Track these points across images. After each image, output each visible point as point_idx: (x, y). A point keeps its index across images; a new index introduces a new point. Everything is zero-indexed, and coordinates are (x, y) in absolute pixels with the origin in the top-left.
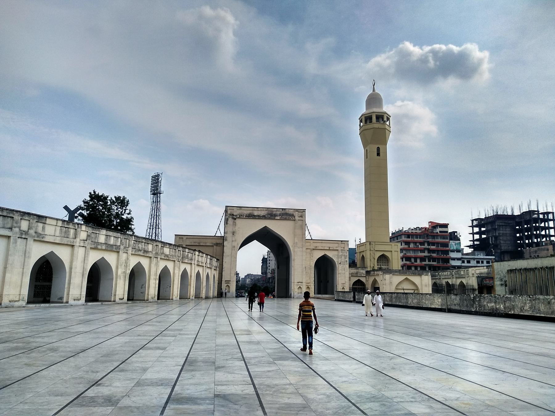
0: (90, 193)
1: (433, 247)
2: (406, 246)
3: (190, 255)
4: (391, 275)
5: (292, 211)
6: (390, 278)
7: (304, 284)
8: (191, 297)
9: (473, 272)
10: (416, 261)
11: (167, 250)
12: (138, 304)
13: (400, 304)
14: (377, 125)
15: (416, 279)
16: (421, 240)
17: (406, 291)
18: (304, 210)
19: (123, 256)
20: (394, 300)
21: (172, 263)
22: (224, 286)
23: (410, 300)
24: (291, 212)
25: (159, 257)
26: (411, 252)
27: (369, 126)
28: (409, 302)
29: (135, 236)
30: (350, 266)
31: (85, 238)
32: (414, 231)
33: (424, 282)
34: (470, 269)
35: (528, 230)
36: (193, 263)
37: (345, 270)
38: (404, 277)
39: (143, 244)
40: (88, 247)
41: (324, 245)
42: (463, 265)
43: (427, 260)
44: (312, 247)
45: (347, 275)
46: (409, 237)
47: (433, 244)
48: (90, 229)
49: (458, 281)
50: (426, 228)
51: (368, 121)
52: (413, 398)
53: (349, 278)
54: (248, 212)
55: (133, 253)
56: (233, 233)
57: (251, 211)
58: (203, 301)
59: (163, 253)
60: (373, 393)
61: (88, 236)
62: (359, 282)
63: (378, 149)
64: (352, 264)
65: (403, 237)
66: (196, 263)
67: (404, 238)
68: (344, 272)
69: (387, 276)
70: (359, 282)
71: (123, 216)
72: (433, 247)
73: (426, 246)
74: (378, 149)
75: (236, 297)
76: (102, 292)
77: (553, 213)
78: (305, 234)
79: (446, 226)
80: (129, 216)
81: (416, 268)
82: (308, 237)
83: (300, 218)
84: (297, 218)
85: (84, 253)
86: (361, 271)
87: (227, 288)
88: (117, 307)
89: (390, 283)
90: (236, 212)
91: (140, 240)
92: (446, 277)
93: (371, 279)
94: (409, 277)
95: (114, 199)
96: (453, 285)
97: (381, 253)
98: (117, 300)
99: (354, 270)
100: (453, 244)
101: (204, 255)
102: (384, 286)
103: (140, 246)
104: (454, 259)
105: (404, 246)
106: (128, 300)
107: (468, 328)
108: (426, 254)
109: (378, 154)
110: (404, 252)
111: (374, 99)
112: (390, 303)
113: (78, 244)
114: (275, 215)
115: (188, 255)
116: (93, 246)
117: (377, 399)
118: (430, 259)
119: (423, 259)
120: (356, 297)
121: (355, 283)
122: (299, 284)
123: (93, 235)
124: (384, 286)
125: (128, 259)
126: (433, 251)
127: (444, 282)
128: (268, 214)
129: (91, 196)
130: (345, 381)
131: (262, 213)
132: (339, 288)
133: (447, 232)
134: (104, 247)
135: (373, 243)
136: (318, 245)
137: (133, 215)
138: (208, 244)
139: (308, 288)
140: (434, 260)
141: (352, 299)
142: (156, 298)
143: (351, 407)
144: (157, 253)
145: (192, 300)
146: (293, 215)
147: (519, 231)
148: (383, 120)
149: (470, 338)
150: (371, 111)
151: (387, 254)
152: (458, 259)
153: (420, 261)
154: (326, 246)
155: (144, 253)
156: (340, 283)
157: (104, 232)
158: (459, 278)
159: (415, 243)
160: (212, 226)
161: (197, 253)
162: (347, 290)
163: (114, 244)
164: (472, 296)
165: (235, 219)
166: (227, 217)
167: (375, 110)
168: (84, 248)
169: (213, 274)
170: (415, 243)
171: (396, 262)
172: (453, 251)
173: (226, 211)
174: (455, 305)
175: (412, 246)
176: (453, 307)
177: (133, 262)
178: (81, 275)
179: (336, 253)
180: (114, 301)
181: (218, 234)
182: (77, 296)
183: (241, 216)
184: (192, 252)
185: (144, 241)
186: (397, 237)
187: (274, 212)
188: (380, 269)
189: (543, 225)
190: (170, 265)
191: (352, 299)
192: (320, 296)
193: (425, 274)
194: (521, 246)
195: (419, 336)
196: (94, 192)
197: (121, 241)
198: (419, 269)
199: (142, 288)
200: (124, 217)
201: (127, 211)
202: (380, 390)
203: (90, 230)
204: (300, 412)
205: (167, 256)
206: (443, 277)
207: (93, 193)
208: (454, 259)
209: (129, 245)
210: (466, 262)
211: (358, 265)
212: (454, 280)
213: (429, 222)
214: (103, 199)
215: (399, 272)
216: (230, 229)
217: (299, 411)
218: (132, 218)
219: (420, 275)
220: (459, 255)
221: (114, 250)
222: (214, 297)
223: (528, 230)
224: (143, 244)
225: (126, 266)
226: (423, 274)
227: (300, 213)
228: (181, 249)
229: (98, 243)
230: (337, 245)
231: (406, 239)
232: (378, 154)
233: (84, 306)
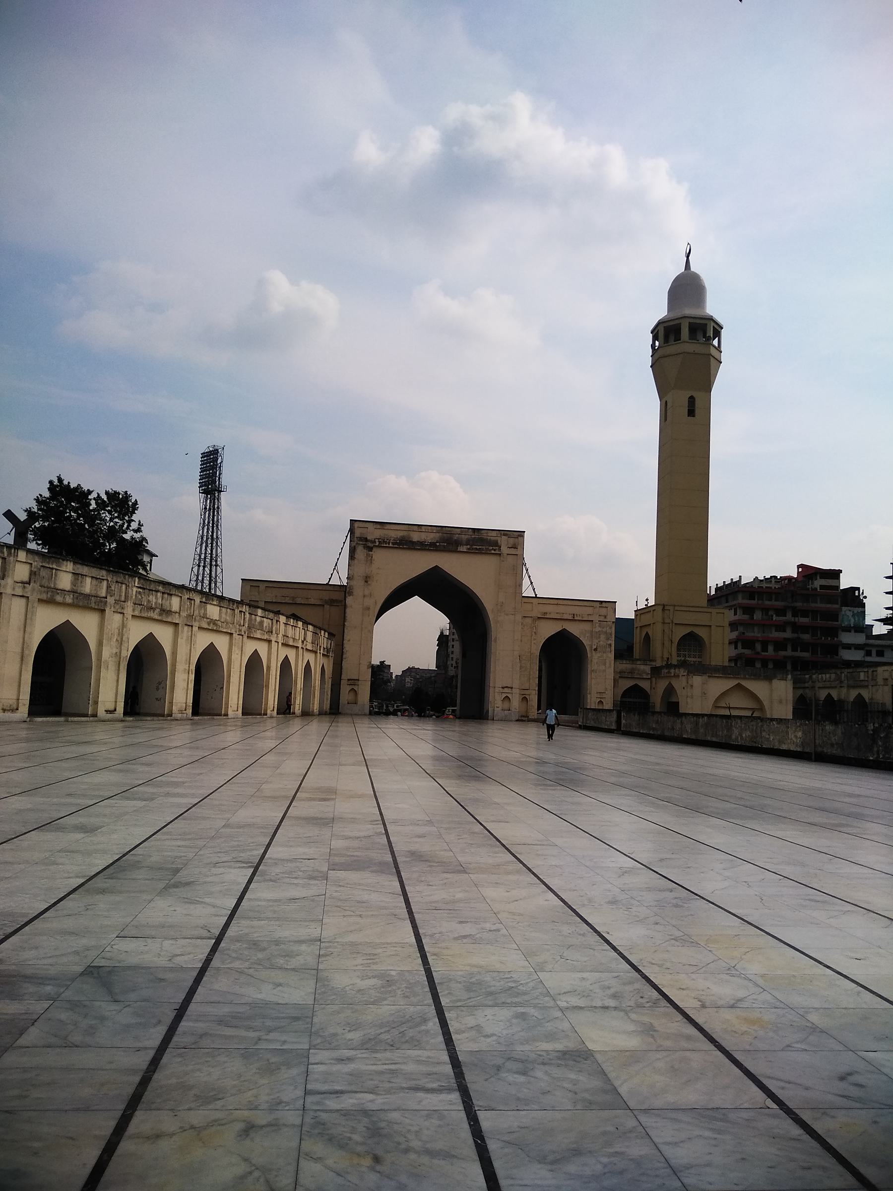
0: (51, 482)
1: (804, 620)
2: (746, 617)
3: (266, 622)
4: (705, 677)
5: (494, 534)
6: (703, 684)
7: (516, 691)
8: (269, 712)
9: (886, 675)
10: (765, 649)
11: (213, 611)
12: (149, 723)
13: (714, 739)
14: (691, 347)
15: (758, 687)
16: (779, 604)
17: (735, 713)
18: (521, 534)
19: (114, 620)
20: (702, 730)
21: (226, 638)
22: (345, 689)
23: (736, 732)
24: (492, 537)
25: (196, 625)
26: (756, 629)
27: (673, 348)
28: (734, 737)
29: (141, 577)
30: (619, 656)
31: (26, 579)
32: (764, 585)
33: (777, 695)
34: (880, 669)
36: (273, 639)
37: (605, 664)
38: (731, 683)
39: (159, 594)
40: (34, 597)
41: (561, 609)
42: (868, 659)
43: (789, 648)
44: (536, 613)
45: (610, 674)
46: (752, 597)
47: (805, 613)
48: (37, 558)
49: (853, 694)
50: (789, 579)
51: (672, 338)
52: (614, 996)
53: (615, 681)
54: (400, 534)
55: (137, 613)
56: (367, 579)
57: (405, 533)
58: (270, 720)
59: (205, 616)
60: (515, 976)
61: (32, 574)
62: (635, 691)
63: (692, 400)
64: (623, 652)
65: (740, 596)
66: (280, 641)
67: (740, 600)
68: (602, 668)
69: (697, 680)
70: (635, 691)
71: (124, 536)
72: (804, 620)
73: (789, 617)
74: (692, 400)
75: (319, 714)
76: (70, 697)
78: (521, 585)
79: (835, 574)
80: (137, 536)
81: (765, 663)
82: (527, 592)
83: (512, 551)
84: (504, 550)
85: (23, 610)
86: (642, 667)
87: (352, 694)
88: (101, 727)
89: (700, 694)
90: (374, 534)
91: (152, 587)
92: (828, 684)
93: (662, 685)
94: (745, 683)
95: (105, 498)
96: (841, 701)
97: (687, 630)
98: (101, 712)
99: (625, 666)
100: (847, 614)
101: (300, 624)
102: (689, 700)
103: (152, 598)
104: (848, 647)
105: (740, 616)
106: (126, 713)
107: (847, 800)
108: (788, 634)
109: (691, 413)
110: (741, 629)
111: (687, 288)
112: (693, 737)
113: (9, 591)
114: (458, 543)
115: (261, 623)
116: (44, 596)
117: (518, 995)
118: (797, 644)
119: (780, 645)
120: (623, 722)
121: (627, 693)
122: (506, 690)
123: (43, 573)
124: (689, 700)
125: (123, 625)
126: (805, 629)
127: (822, 695)
128: (442, 540)
129: (52, 487)
130: (465, 937)
131: (430, 537)
132: (592, 702)
133: (838, 587)
134: (69, 599)
135: (671, 608)
136: (549, 609)
137: (145, 533)
138: (312, 601)
139: (525, 699)
140: (805, 647)
141: (614, 727)
142: (190, 711)
143: (425, 1021)
144: (190, 616)
145: (271, 717)
146: (496, 544)
148: (705, 336)
149: (837, 825)
150: (677, 314)
151: (697, 631)
152: (858, 647)
153: (775, 650)
154: (567, 612)
155: (160, 615)
157: (69, 566)
158: (854, 687)
159: (765, 610)
160: (323, 562)
161: (283, 619)
162: (608, 705)
163: (93, 593)
164: (871, 727)
165: (371, 549)
166: (354, 544)
167: (688, 312)
168: (23, 601)
169: (318, 662)
170: (765, 610)
171: (720, 650)
172: (848, 629)
173: (352, 531)
174: (832, 745)
175: (758, 616)
176: (828, 750)
177: (137, 632)
178: (18, 659)
179: (587, 627)
180: (95, 715)
181: (335, 581)
182: (11, 702)
183: (383, 543)
184: (271, 615)
185: (160, 588)
186: (727, 595)
187: (456, 537)
188: (683, 664)
190: (221, 643)
191: (614, 727)
195: (723, 816)
196: (60, 480)
197: (108, 587)
198: (771, 666)
199: (158, 689)
200: (127, 536)
201: (134, 525)
202: (540, 968)
203: (37, 562)
204: (272, 1036)
205: (214, 622)
206: (820, 685)
207: (56, 482)
208: (848, 647)
209: (126, 597)
210: (874, 653)
211: (636, 655)
212: (844, 690)
213: (799, 567)
214: (80, 495)
215: (722, 672)
216: (361, 570)
217: (270, 1031)
218: (144, 539)
219: (769, 679)
220: (860, 639)
221: (93, 605)
222: (321, 713)
224: (159, 594)
225: (120, 642)
226: (775, 677)
227: (511, 541)
228: (244, 608)
229: (56, 591)
230: (589, 610)
231: (745, 601)
232: (691, 413)
233: (24, 725)
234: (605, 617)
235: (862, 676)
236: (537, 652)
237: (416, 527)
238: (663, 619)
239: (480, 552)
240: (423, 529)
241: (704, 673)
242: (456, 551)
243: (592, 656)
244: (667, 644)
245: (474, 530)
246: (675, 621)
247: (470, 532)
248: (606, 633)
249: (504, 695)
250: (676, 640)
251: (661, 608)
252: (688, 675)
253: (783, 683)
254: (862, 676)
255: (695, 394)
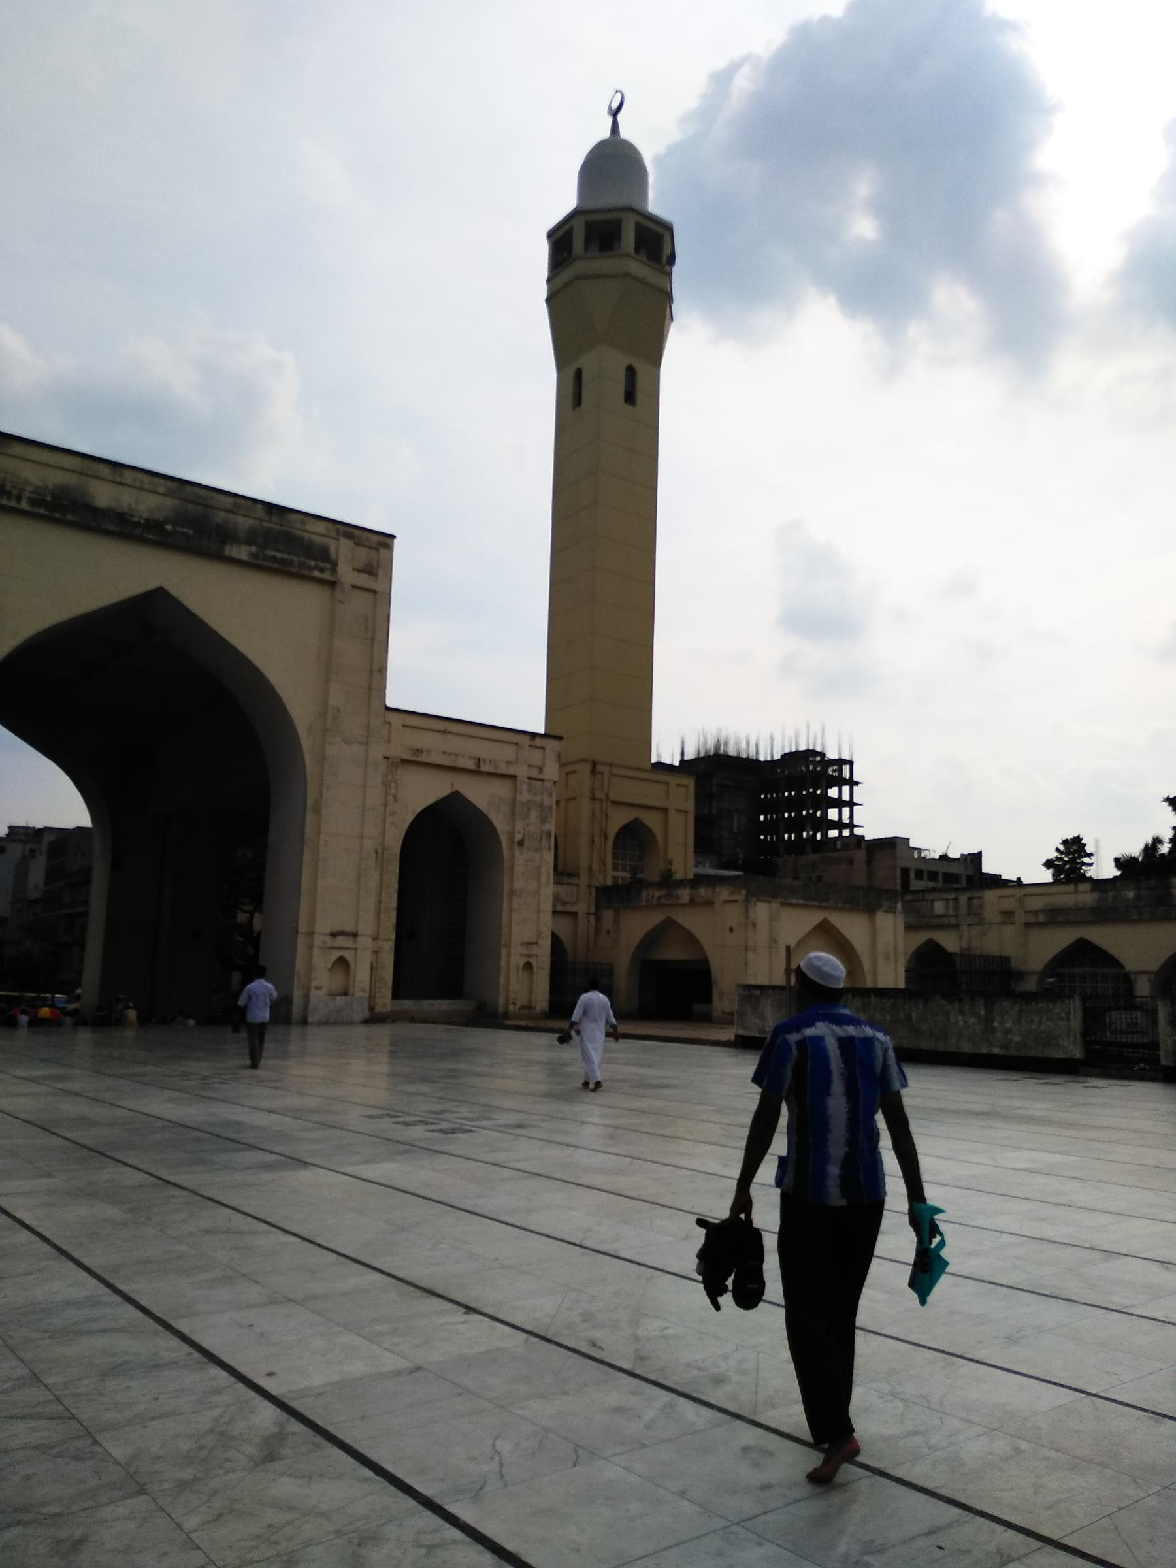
4: (776, 905)
6: (772, 919)
15: (852, 926)
35: (791, 804)
38: (811, 919)
44: (398, 750)
54: (55, 479)
57: (70, 480)
63: (631, 371)
68: (532, 886)
74: (631, 371)
77: (851, 763)
109: (630, 397)
114: (226, 535)
131: (147, 505)
136: (427, 741)
147: (766, 807)
156: (516, 940)
179: (501, 789)
187: (220, 517)
189: (833, 792)
192: (408, 1004)
193: (886, 904)
194: (773, 849)
219: (870, 909)
223: (791, 804)
230: (509, 752)
232: (630, 397)
234: (541, 770)
235: (939, 907)
236: (395, 843)
237: (105, 471)
238: (593, 790)
239: (282, 570)
240: (128, 476)
241: (775, 897)
242: (219, 557)
243: (513, 857)
244: (597, 839)
245: (270, 508)
246: (612, 797)
247: (260, 511)
248: (541, 805)
249: (335, 955)
250: (612, 832)
251: (588, 767)
252: (747, 900)
253: (890, 916)
254: (939, 907)
255: (639, 365)
